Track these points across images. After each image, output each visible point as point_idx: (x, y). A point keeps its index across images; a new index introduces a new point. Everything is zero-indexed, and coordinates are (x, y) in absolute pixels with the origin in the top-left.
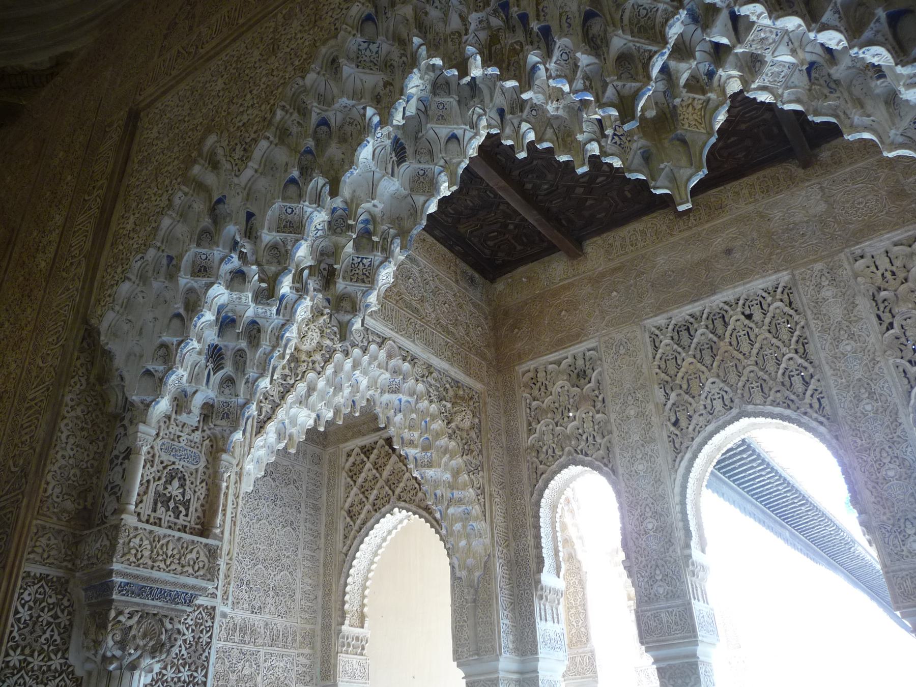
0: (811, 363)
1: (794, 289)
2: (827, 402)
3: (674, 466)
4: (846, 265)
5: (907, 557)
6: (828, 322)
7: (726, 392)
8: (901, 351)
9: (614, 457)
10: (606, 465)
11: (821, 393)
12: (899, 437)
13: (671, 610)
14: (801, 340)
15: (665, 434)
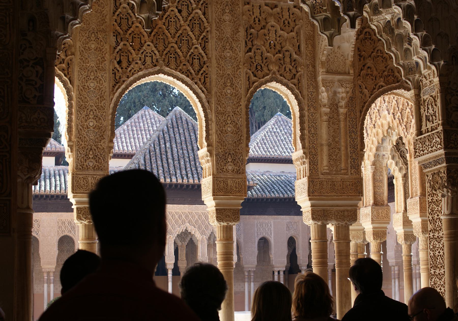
0: (206, 55)
1: (209, 6)
2: (209, 81)
3: (113, 90)
4: (240, 6)
5: (225, 172)
6: (223, 35)
8: (251, 66)
9: (73, 72)
10: (65, 76)
11: (206, 74)
12: (238, 111)
13: (95, 176)
14: (205, 39)
15: (111, 68)
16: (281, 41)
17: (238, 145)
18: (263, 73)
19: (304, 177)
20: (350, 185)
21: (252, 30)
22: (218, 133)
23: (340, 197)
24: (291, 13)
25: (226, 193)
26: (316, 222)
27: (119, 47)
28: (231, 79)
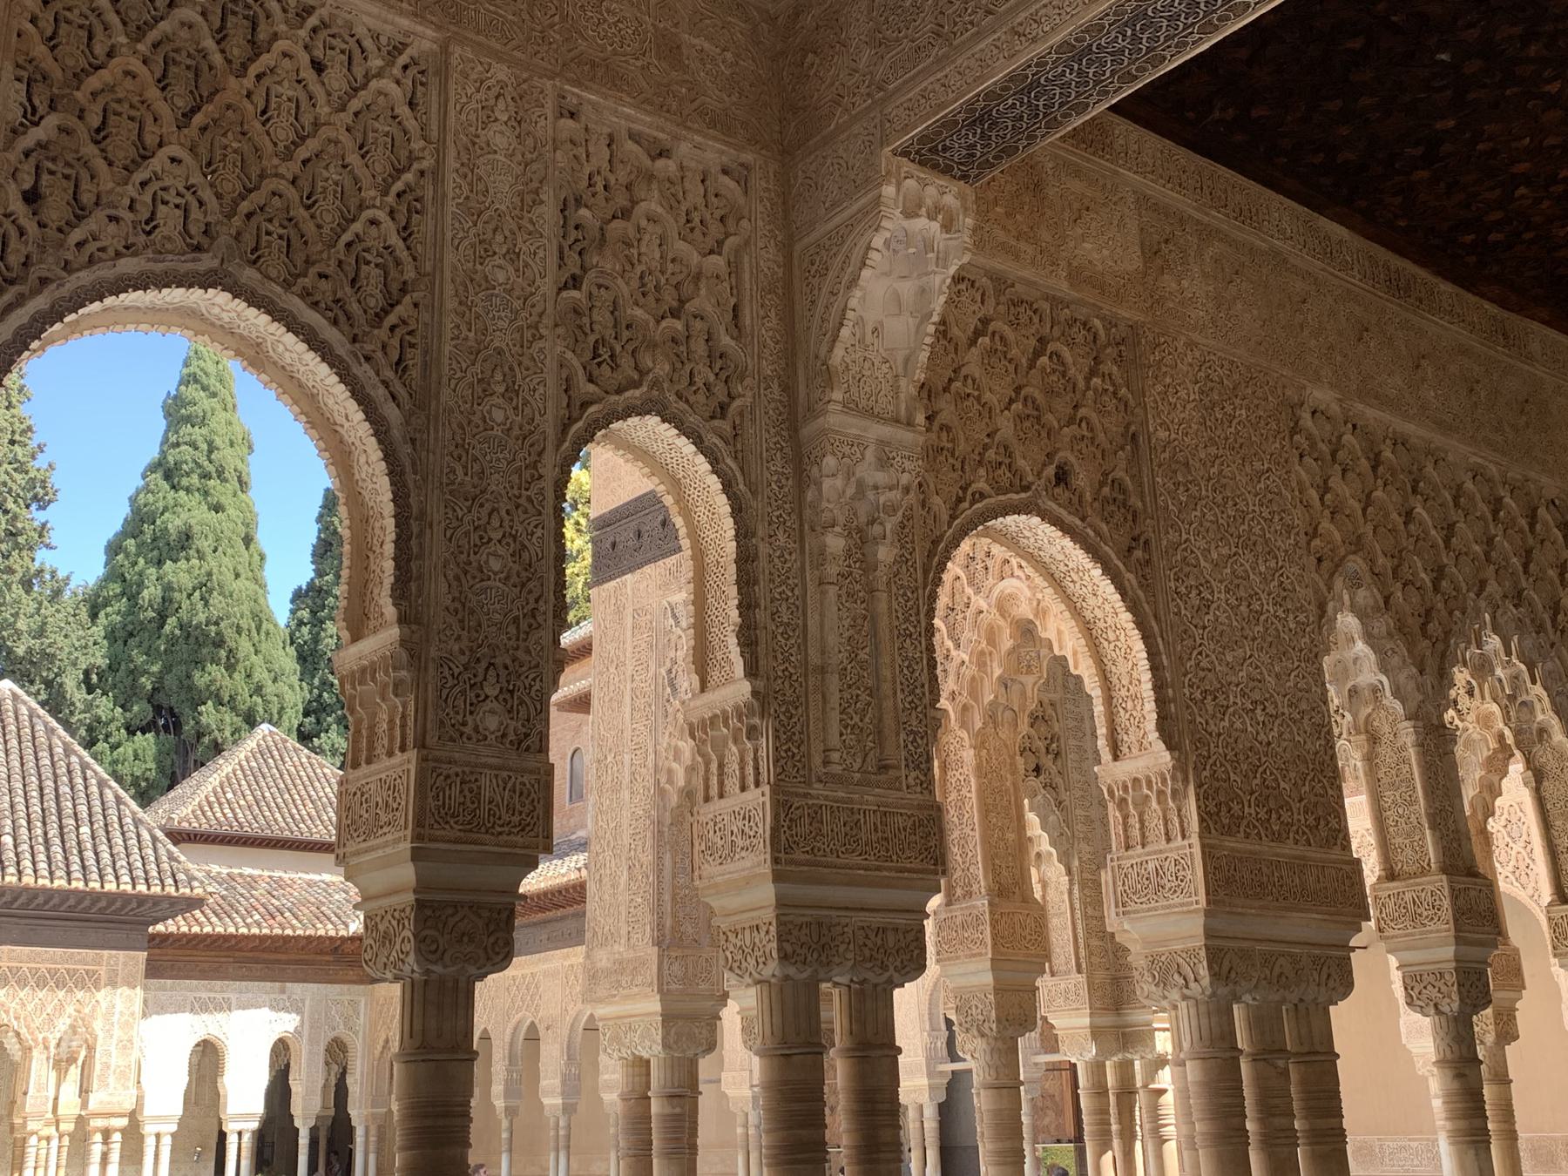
0: (415, 259)
1: (434, 81)
2: (418, 360)
7: (201, 204)
11: (410, 333)
12: (529, 499)
16: (680, 277)
17: (528, 633)
18: (619, 377)
19: (743, 788)
20: (905, 830)
21: (583, 212)
22: (451, 574)
23: (877, 873)
24: (711, 191)
25: (471, 831)
26: (792, 971)
27: (36, 134)
28: (506, 369)
